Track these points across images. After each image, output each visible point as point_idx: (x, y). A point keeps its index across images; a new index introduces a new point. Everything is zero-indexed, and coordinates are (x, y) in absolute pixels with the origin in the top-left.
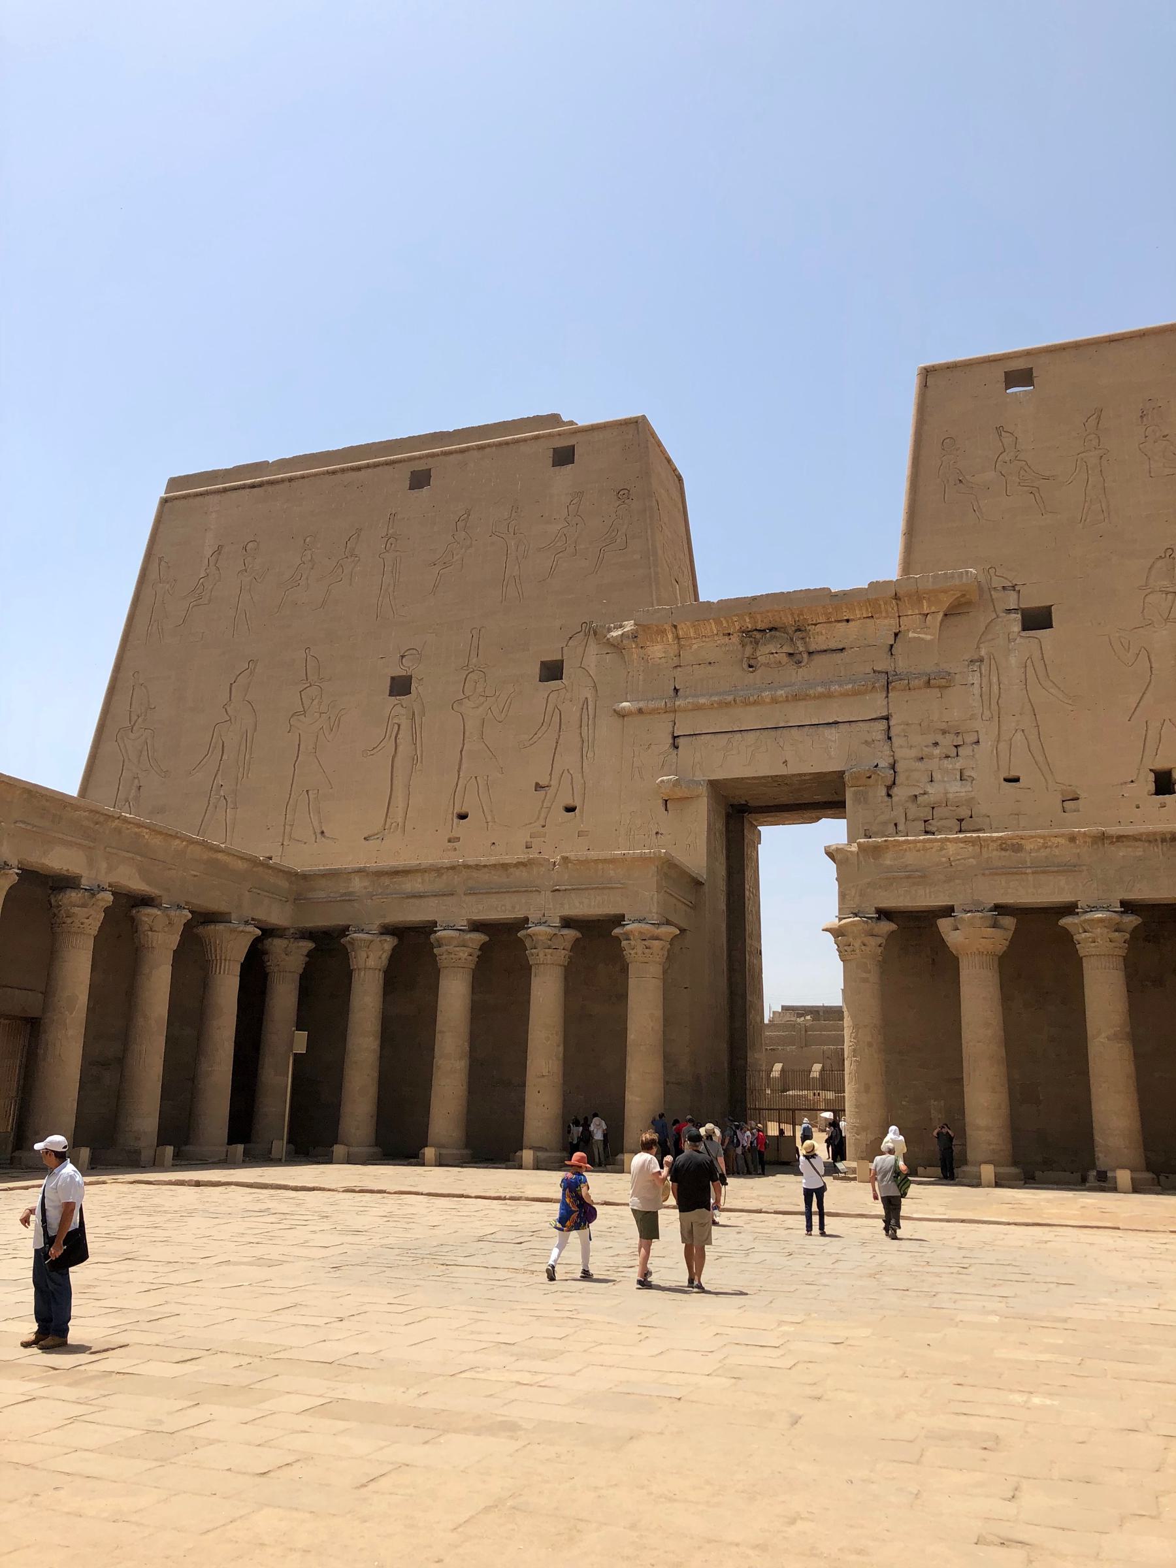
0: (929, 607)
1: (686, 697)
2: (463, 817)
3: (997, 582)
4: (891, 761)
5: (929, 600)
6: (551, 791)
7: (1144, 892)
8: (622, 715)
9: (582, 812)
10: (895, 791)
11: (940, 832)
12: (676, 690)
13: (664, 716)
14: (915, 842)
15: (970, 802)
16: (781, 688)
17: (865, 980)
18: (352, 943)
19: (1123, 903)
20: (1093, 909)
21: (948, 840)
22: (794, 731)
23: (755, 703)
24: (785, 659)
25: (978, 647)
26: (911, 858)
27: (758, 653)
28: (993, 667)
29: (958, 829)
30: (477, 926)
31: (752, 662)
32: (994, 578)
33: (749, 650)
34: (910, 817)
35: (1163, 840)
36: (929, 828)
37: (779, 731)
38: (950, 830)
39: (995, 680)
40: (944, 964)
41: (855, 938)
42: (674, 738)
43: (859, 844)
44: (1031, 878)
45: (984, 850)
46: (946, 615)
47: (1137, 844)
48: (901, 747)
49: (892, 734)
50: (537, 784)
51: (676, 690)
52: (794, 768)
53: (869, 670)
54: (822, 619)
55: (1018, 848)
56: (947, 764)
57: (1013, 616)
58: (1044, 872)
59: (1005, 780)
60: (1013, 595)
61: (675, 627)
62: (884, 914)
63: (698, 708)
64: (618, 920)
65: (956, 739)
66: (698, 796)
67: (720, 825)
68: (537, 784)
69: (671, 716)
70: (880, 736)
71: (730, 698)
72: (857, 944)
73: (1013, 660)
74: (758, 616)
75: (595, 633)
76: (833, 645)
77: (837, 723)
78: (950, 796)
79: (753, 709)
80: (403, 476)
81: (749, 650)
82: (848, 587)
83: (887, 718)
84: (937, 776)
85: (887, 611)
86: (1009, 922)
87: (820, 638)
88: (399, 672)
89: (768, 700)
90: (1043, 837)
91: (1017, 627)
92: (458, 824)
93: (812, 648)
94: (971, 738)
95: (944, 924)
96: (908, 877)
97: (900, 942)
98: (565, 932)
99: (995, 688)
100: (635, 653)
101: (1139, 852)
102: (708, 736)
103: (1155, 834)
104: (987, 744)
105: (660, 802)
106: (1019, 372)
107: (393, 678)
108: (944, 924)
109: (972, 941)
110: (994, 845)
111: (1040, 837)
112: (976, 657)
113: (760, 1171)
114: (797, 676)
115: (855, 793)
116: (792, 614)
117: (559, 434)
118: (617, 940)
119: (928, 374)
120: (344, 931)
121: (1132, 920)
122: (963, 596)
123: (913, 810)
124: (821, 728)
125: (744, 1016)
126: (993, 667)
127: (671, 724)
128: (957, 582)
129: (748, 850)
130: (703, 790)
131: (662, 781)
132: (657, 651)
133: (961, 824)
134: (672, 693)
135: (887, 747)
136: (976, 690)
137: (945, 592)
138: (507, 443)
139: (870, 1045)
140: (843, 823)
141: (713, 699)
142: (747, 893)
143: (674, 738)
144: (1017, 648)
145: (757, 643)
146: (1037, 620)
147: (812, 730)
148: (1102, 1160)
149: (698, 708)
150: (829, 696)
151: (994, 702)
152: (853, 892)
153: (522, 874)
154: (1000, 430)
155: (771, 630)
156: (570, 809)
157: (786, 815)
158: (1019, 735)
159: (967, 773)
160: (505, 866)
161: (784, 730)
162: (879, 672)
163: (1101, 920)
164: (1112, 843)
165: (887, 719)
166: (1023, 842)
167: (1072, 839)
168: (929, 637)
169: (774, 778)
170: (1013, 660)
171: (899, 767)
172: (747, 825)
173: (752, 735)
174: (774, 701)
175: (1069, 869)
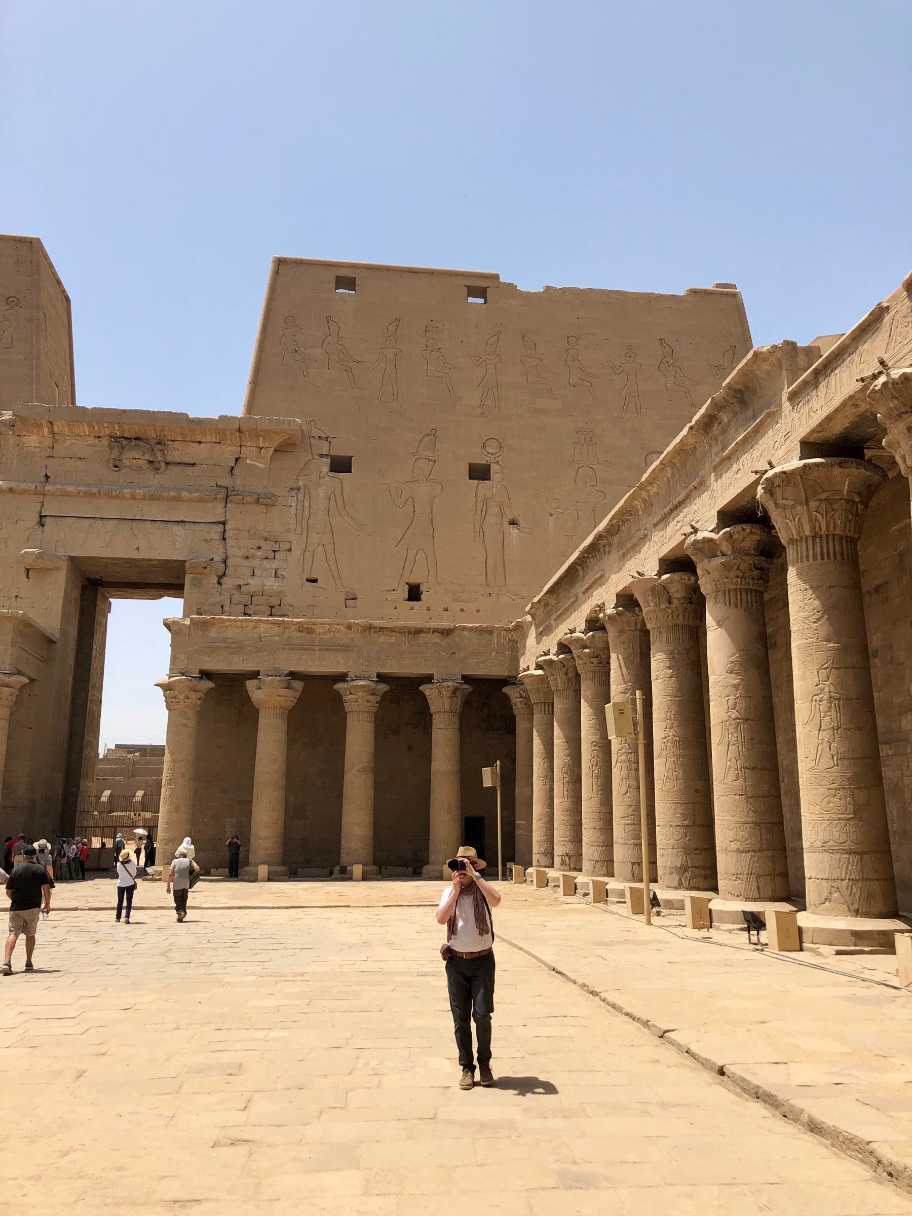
0: (264, 441)
1: (57, 484)
4: (224, 557)
5: (264, 438)
7: (392, 668)
10: (225, 580)
11: (255, 614)
13: (35, 497)
14: (235, 621)
15: (280, 594)
16: (140, 488)
17: (186, 725)
19: (378, 675)
20: (358, 678)
21: (260, 621)
22: (148, 524)
23: (116, 497)
24: (146, 465)
25: (297, 479)
26: (230, 633)
28: (307, 495)
29: (269, 613)
31: (117, 463)
32: (314, 429)
33: (115, 454)
34: (234, 601)
35: (409, 633)
36: (248, 611)
37: (135, 523)
38: (263, 615)
39: (307, 505)
40: (248, 715)
41: (180, 693)
42: (41, 517)
43: (191, 619)
44: (318, 653)
45: (287, 631)
46: (276, 451)
47: (392, 634)
48: (233, 547)
49: (227, 535)
52: (145, 554)
53: (213, 484)
55: (311, 631)
56: (266, 563)
57: (325, 459)
58: (327, 650)
59: (308, 580)
60: (326, 444)
61: (51, 423)
62: (206, 675)
63: (66, 494)
66: (58, 569)
67: (76, 594)
71: (95, 490)
72: (182, 697)
73: (321, 492)
74: (126, 426)
76: (186, 459)
77: (183, 522)
78: (266, 588)
79: (115, 501)
82: (202, 416)
83: (224, 523)
85: (231, 440)
86: (298, 685)
87: (177, 453)
89: (128, 496)
90: (329, 624)
91: (326, 469)
94: (285, 546)
95: (250, 684)
96: (227, 647)
97: (214, 697)
99: (307, 511)
101: (393, 640)
103: (405, 627)
104: (297, 551)
106: (347, 278)
108: (250, 684)
109: (270, 698)
110: (293, 628)
111: (327, 624)
112: (295, 486)
113: (81, 877)
114: (155, 480)
115: (193, 579)
116: (155, 429)
119: (280, 264)
121: (383, 687)
122: (290, 438)
124: (170, 525)
125: (81, 752)
126: (307, 495)
127: (40, 505)
128: (286, 427)
129: (98, 617)
130: (64, 564)
131: (26, 553)
132: (32, 441)
133: (272, 610)
134: (43, 479)
135: (221, 546)
136: (293, 511)
139: (183, 775)
140: (180, 602)
141: (80, 488)
142: (94, 652)
143: (41, 517)
144: (327, 484)
145: (123, 448)
146: (341, 465)
147: (163, 525)
148: (345, 859)
149: (66, 494)
150: (179, 499)
151: (304, 522)
152: (183, 656)
154: (328, 319)
155: (137, 439)
157: (134, 591)
158: (320, 548)
159: (280, 572)
161: (140, 524)
162: (221, 487)
163: (362, 686)
164: (376, 632)
165: (224, 523)
166: (315, 627)
167: (349, 627)
168: (261, 466)
169: (127, 561)
170: (321, 492)
171: (229, 562)
172: (99, 596)
173: (111, 522)
175: (346, 648)
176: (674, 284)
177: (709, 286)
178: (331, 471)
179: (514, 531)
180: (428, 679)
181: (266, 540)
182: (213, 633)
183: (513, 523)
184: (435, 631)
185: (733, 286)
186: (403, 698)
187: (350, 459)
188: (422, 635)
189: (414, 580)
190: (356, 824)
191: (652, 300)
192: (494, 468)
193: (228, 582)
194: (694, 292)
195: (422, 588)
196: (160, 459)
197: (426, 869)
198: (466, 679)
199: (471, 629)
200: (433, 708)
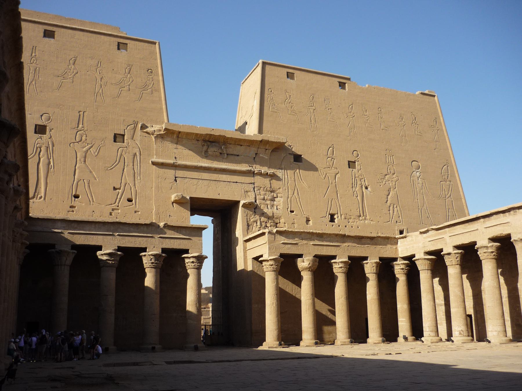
2: (76, 197)
6: (120, 191)
8: (154, 163)
10: (257, 210)
12: (176, 158)
18: (60, 252)
27: (209, 150)
37: (217, 182)
42: (176, 177)
50: (114, 188)
51: (176, 158)
54: (233, 143)
62: (282, 255)
66: (186, 203)
68: (114, 188)
75: (141, 127)
80: (42, 28)
81: (205, 148)
87: (233, 149)
88: (40, 123)
91: (292, 160)
92: (75, 200)
93: (228, 152)
102: (190, 179)
107: (36, 125)
120: (53, 246)
137: (276, 143)
143: (176, 177)
145: (208, 146)
154: (286, 91)
156: (130, 200)
168: (266, 157)
178: (295, 161)
181: (272, 191)
183: (366, 188)
188: (363, 239)
195: (336, 217)
196: (225, 152)
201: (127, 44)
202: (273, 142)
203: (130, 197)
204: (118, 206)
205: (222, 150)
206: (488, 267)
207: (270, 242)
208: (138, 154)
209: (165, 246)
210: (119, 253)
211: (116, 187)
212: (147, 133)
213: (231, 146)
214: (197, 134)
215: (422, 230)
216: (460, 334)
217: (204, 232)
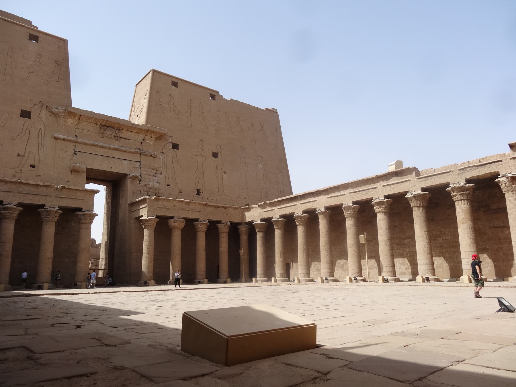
3: (168, 135)
8: (56, 138)
9: (38, 168)
15: (159, 189)
20: (204, 221)
22: (114, 159)
30: (20, 205)
50: (18, 154)
56: (154, 178)
61: (81, 116)
62: (158, 217)
64: (80, 210)
65: (157, 172)
68: (18, 154)
69: (74, 144)
70: (138, 166)
72: (152, 224)
75: (47, 107)
81: (102, 131)
83: (140, 162)
84: (151, 180)
91: (171, 147)
93: (121, 136)
98: (59, 211)
100: (62, 118)
105: (70, 171)
106: (175, 82)
109: (177, 225)
117: (33, 30)
118: (77, 215)
119: (154, 71)
123: (145, 189)
137: (160, 133)
138: (8, 21)
144: (171, 152)
147: (120, 160)
149: (84, 144)
150: (125, 151)
153: (44, 189)
154: (170, 95)
156: (33, 166)
160: (37, 185)
167: (200, 204)
174: (109, 148)
176: (263, 106)
177: (270, 108)
179: (225, 176)
180: (220, 222)
181: (153, 169)
182: (160, 203)
183: (224, 173)
184: (223, 207)
185: (276, 110)
186: (213, 227)
187: (178, 145)
189: (198, 188)
190: (201, 266)
191: (257, 109)
192: (219, 154)
193: (142, 183)
194: (267, 109)
195: (201, 191)
197: (220, 280)
198: (231, 223)
199: (233, 208)
200: (220, 231)
201: (38, 37)
202: (157, 132)
203: (32, 163)
204: (21, 170)
205: (116, 134)
206: (300, 231)
207: (149, 207)
208: (42, 129)
209: (61, 204)
210: (18, 208)
211: (20, 154)
212: (52, 112)
213: (123, 131)
214: (95, 119)
215: (260, 204)
216: (281, 276)
217: (96, 196)
